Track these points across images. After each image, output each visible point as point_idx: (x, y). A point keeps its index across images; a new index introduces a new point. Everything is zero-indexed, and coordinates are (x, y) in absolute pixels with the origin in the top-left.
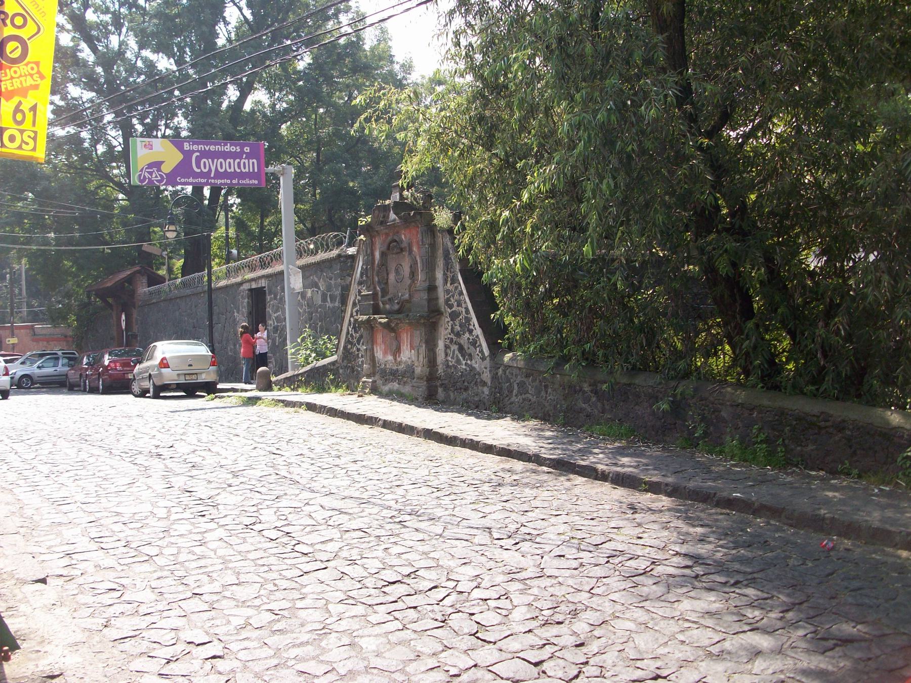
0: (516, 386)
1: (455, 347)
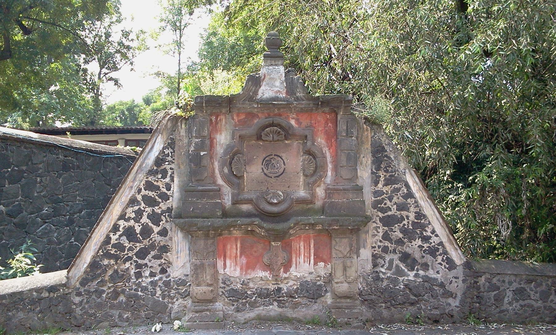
0: (509, 294)
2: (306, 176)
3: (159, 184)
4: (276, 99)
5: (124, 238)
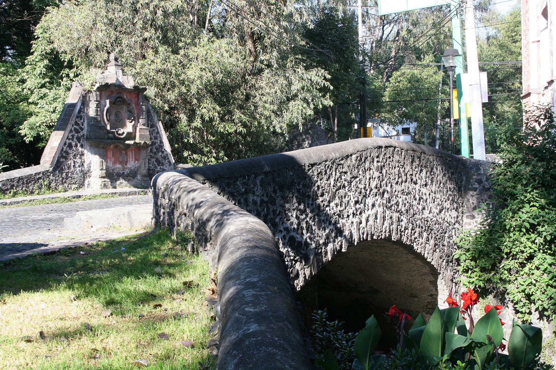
1: (154, 160)
3: (80, 122)
5: (68, 148)
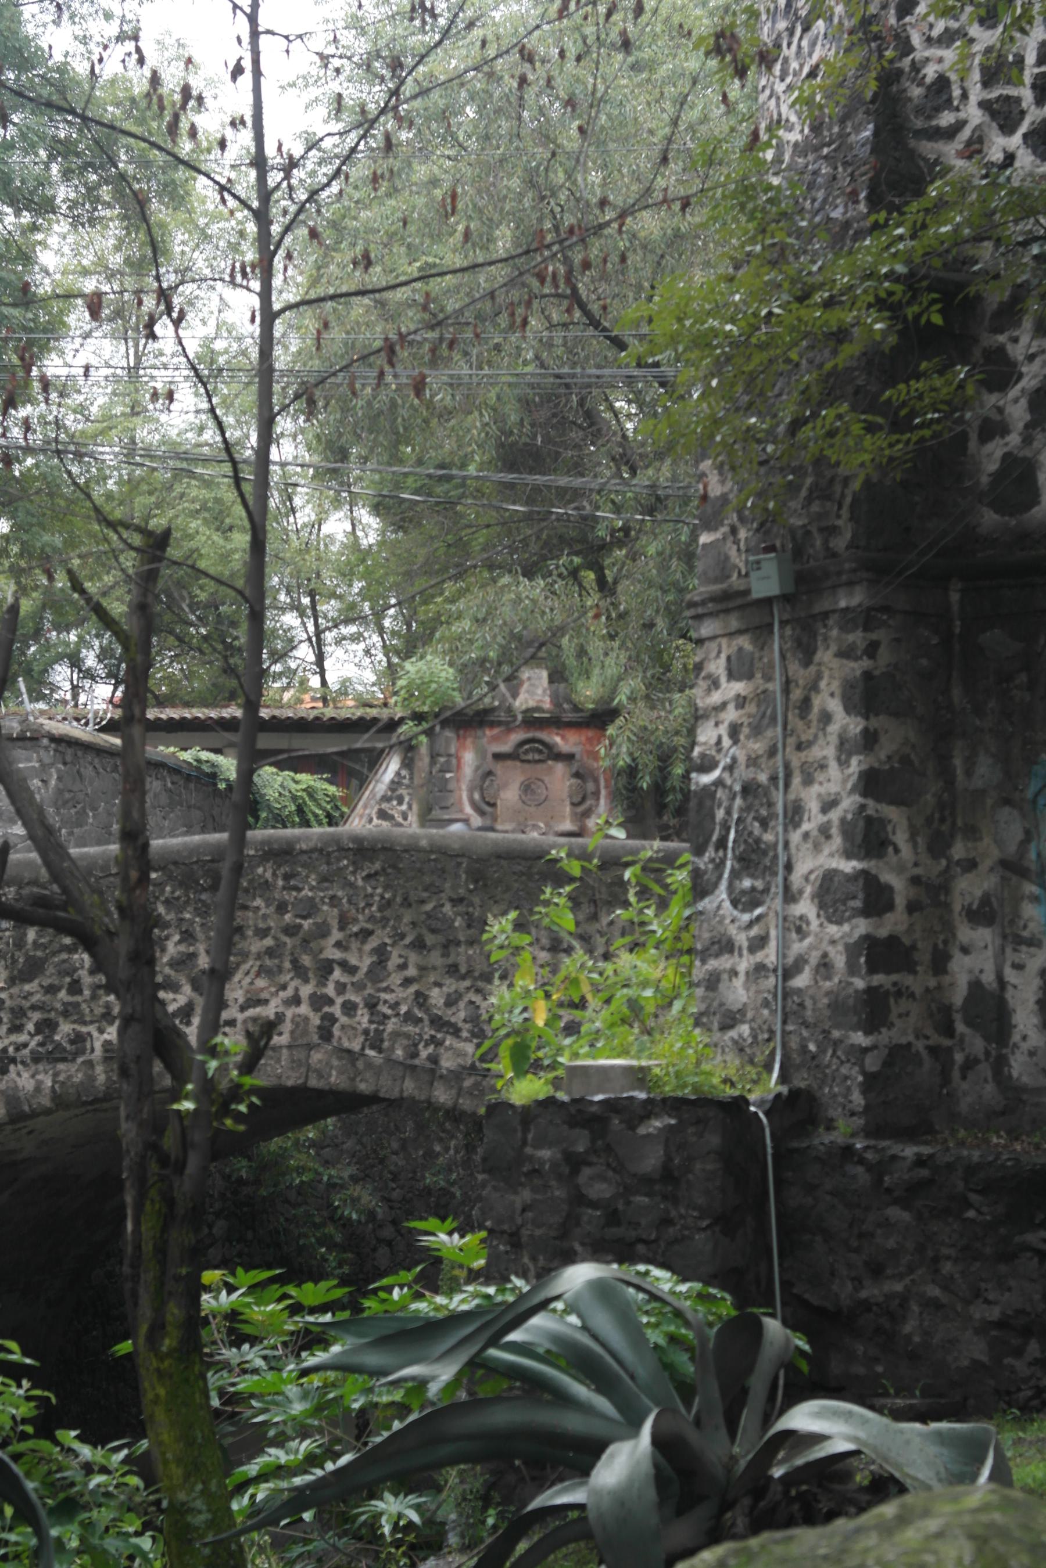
2: (573, 804)
4: (538, 709)
